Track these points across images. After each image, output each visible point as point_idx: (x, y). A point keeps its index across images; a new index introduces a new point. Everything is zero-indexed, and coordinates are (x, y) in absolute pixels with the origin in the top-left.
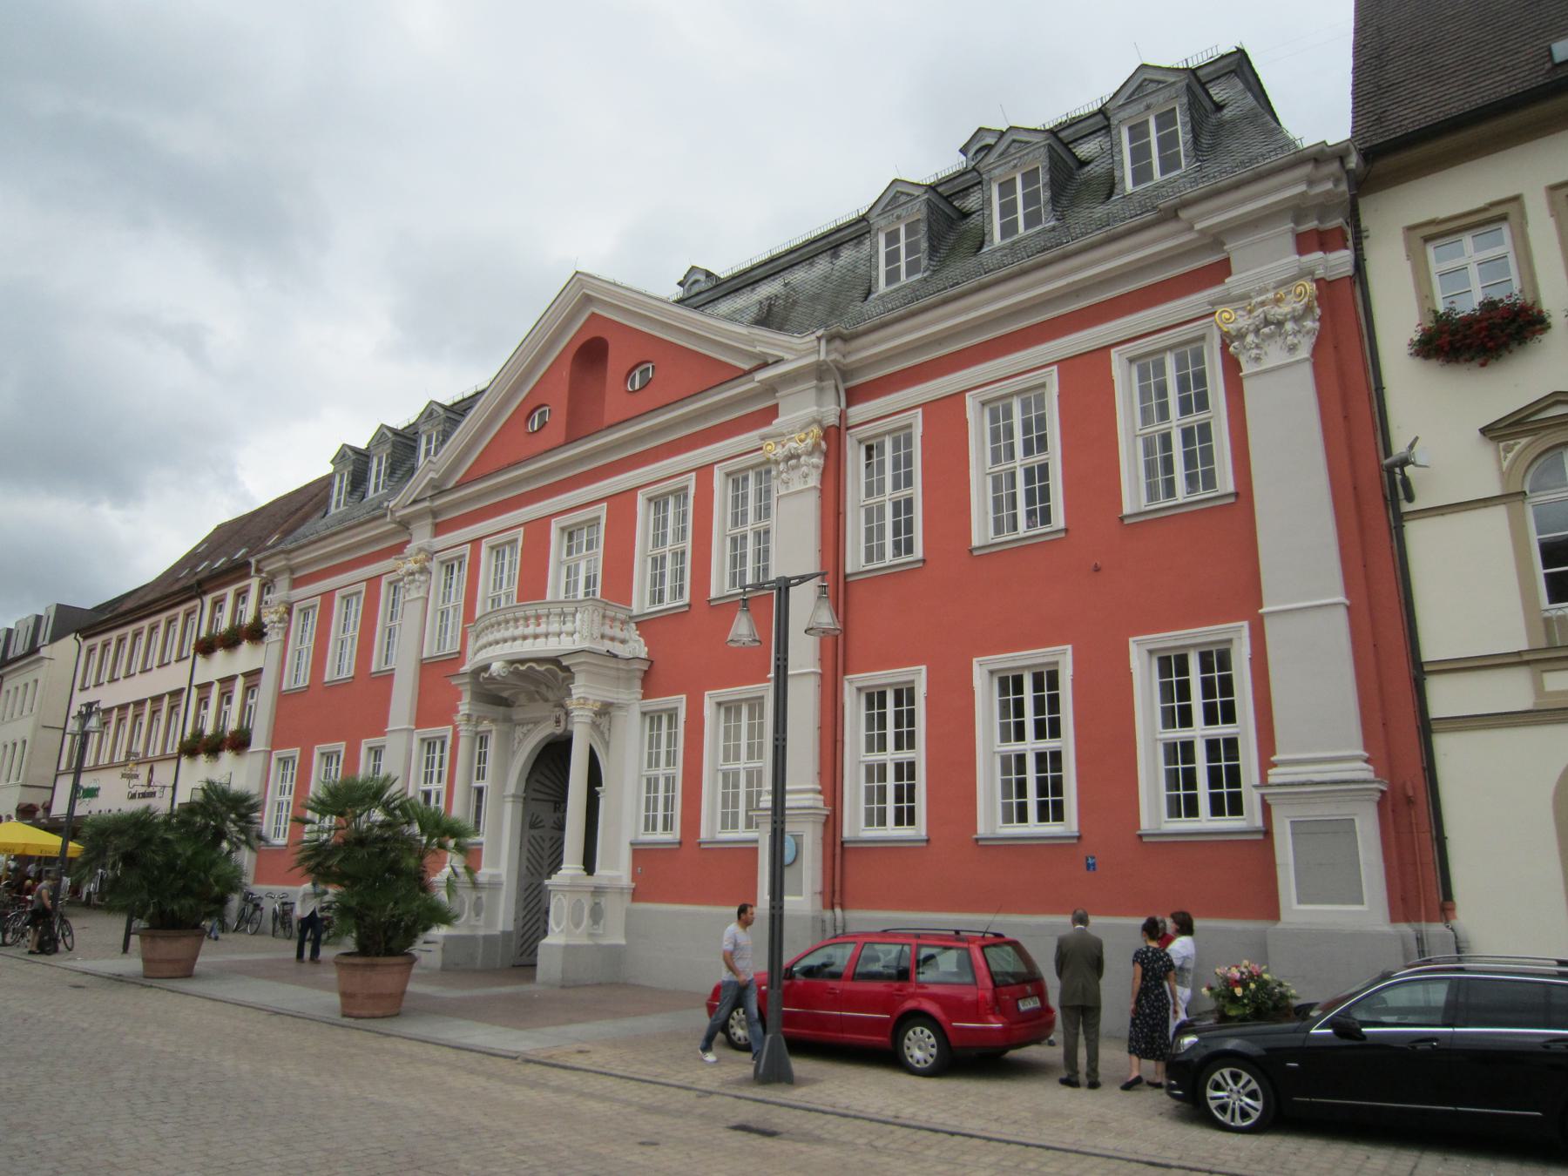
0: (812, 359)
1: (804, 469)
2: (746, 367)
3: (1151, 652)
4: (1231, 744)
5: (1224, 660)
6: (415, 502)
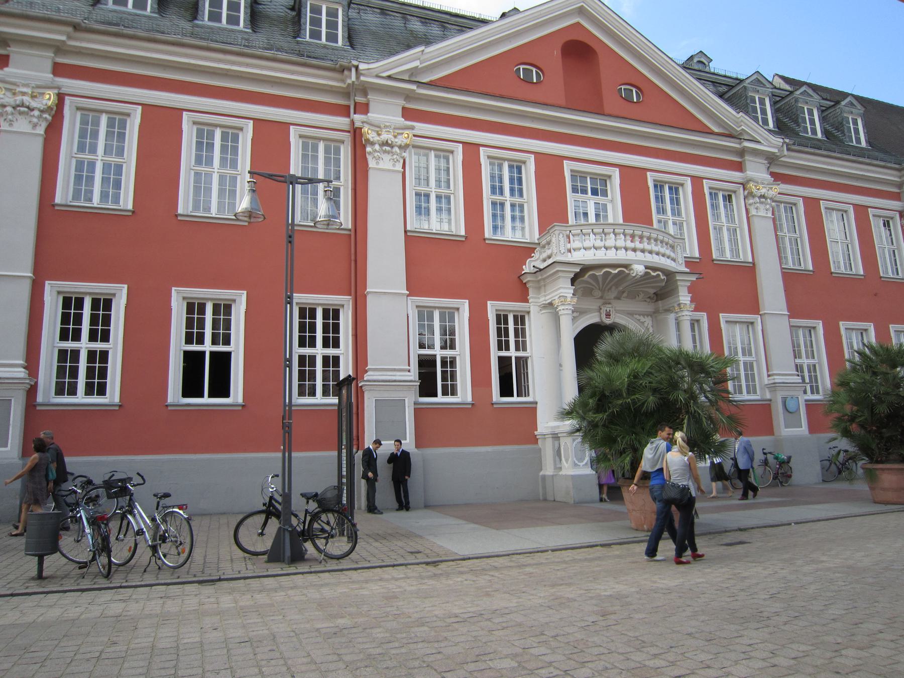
0: (776, 151)
1: (768, 206)
2: (716, 130)
3: (59, 293)
4: (104, 355)
5: (108, 304)
6: (389, 77)
